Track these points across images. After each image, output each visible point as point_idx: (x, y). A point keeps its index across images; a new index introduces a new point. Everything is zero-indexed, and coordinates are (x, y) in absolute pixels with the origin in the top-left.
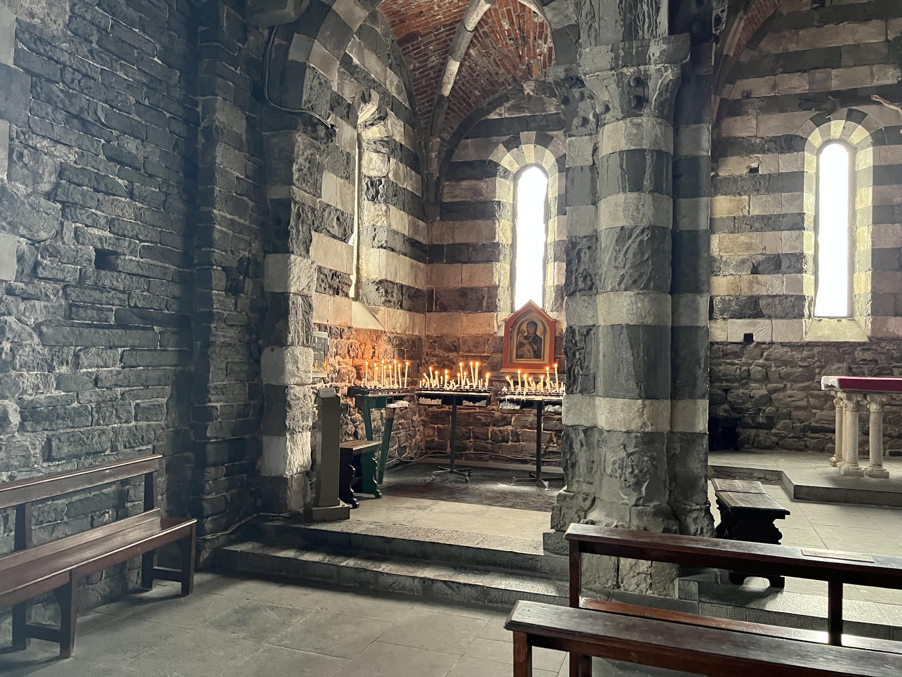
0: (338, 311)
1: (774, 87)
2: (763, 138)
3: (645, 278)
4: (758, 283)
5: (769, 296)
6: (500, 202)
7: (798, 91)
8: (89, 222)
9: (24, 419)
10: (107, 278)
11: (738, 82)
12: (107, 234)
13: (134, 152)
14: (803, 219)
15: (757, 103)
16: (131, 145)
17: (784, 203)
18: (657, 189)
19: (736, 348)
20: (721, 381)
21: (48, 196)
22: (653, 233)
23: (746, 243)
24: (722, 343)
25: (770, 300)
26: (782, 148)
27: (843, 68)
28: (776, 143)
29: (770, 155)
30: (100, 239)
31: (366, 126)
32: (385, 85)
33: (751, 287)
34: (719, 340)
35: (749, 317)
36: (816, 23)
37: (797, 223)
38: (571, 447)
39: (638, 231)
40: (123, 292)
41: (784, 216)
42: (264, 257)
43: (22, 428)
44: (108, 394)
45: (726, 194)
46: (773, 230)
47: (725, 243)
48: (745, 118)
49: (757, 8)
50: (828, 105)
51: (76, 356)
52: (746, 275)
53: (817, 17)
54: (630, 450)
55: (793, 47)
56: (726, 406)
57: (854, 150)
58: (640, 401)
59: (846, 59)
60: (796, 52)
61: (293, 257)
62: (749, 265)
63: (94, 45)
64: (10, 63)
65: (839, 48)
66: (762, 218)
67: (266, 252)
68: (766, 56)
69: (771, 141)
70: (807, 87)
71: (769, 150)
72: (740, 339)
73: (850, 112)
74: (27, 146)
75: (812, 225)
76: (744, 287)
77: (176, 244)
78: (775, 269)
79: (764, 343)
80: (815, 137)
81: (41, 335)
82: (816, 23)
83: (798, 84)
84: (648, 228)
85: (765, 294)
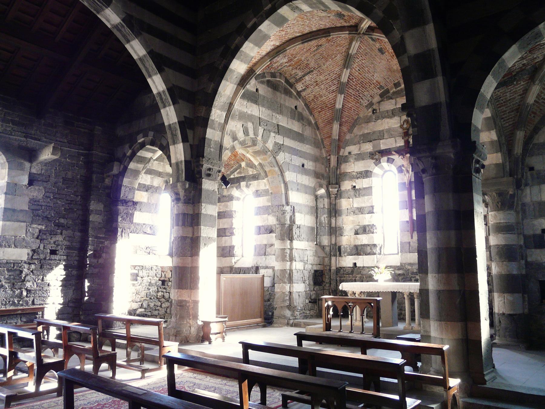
1: (360, 149)
2: (357, 172)
4: (357, 239)
5: (362, 245)
6: (235, 211)
7: (369, 151)
8: (48, 243)
11: (347, 148)
12: (54, 245)
14: (373, 208)
15: (354, 157)
16: (62, 221)
17: (366, 201)
21: (37, 238)
23: (352, 220)
26: (364, 176)
29: (359, 180)
33: (355, 241)
35: (354, 255)
36: (374, 120)
42: (111, 245)
46: (362, 214)
48: (350, 163)
49: (346, 116)
50: (377, 157)
51: (43, 278)
52: (353, 236)
53: (374, 117)
55: (366, 131)
57: (395, 174)
59: (386, 136)
60: (368, 134)
63: (52, 198)
64: (27, 209)
66: (358, 208)
68: (356, 136)
70: (372, 149)
71: (359, 177)
72: (351, 265)
73: (388, 158)
74: (31, 227)
76: (352, 240)
82: (374, 120)
83: (368, 147)
85: (360, 244)
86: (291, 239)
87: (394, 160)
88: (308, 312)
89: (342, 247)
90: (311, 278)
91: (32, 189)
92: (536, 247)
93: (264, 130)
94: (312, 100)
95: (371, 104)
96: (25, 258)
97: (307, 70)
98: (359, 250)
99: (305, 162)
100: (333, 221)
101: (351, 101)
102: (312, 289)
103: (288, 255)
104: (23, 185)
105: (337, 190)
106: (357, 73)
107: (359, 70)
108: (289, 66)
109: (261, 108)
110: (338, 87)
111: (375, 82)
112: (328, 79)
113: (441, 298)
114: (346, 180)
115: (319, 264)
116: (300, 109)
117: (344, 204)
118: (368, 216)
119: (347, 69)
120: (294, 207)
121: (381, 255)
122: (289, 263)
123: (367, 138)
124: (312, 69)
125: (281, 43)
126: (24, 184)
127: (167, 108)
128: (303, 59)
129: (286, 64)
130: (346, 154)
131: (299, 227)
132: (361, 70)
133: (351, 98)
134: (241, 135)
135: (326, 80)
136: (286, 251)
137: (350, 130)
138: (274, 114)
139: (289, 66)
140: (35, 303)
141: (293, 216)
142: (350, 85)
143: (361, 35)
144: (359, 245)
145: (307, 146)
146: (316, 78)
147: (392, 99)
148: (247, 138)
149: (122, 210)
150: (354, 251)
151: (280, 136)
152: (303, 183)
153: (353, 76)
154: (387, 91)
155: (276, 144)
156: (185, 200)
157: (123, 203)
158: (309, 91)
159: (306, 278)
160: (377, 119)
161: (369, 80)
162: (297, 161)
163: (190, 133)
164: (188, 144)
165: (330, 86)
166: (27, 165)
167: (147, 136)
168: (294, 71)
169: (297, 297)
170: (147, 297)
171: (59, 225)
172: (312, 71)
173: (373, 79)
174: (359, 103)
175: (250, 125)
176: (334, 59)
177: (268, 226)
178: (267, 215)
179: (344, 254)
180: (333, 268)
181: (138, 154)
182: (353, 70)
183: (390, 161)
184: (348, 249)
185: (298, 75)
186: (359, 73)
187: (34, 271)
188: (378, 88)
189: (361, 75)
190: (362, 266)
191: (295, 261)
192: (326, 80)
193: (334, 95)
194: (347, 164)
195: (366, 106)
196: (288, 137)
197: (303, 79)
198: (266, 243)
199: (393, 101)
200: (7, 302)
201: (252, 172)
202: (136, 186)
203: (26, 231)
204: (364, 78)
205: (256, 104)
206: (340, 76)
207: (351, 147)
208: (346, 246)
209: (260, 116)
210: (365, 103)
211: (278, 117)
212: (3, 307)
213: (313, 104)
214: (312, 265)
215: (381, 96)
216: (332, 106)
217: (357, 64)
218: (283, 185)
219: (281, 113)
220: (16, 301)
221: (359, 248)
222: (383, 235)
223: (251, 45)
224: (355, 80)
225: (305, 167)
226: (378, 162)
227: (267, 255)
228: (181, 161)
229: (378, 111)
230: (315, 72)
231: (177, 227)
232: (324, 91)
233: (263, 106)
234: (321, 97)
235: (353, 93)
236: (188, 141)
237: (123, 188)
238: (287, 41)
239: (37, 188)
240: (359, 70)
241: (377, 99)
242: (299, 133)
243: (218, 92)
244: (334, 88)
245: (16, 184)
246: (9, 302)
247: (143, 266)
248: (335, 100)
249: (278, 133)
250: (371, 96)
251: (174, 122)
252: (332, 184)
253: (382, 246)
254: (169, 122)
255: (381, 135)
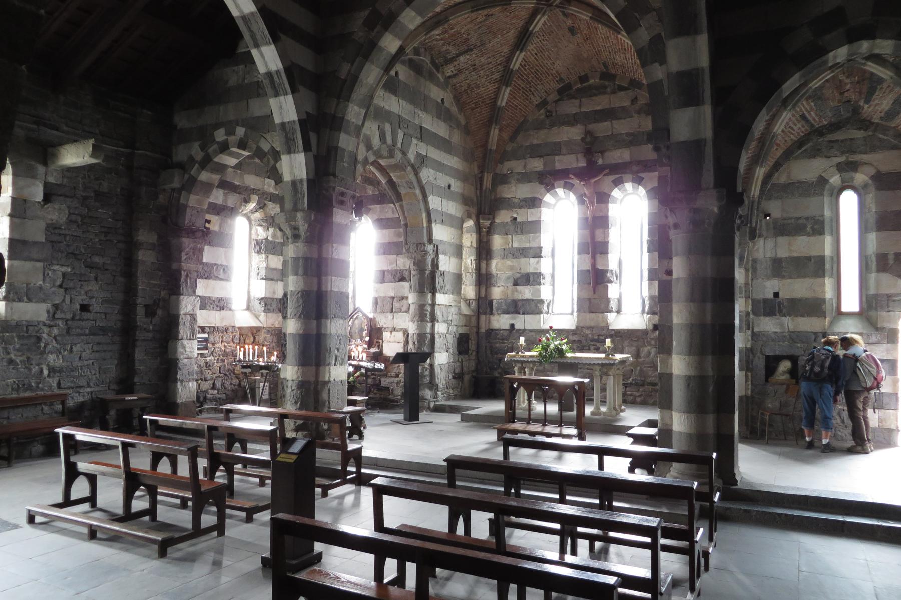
0: (222, 319)
1: (525, 167)
2: (519, 199)
3: (299, 313)
4: (517, 291)
5: (523, 300)
7: (538, 169)
9: (49, 372)
10: (85, 315)
12: (85, 297)
13: (98, 261)
14: (541, 251)
16: (96, 259)
18: (306, 273)
19: (505, 334)
20: (497, 354)
21: (60, 286)
22: (303, 294)
24: (497, 330)
25: (524, 302)
27: (562, 155)
28: (526, 202)
29: (523, 209)
30: (82, 300)
31: (252, 213)
32: (263, 188)
33: (513, 293)
34: (495, 328)
35: (512, 313)
37: (537, 253)
38: (283, 388)
39: (297, 293)
40: (93, 320)
41: (530, 248)
42: (169, 297)
43: (49, 376)
44: (86, 363)
45: (499, 234)
46: (525, 257)
47: (499, 265)
51: (71, 348)
53: (547, 122)
54: (293, 388)
55: (535, 142)
56: (499, 371)
58: (296, 367)
59: (564, 150)
60: (537, 144)
61: (182, 297)
62: (512, 280)
63: (80, 223)
65: (559, 142)
66: (519, 249)
67: (170, 295)
69: (523, 201)
70: (542, 167)
71: (522, 206)
72: (507, 327)
73: (566, 183)
74: (50, 270)
75: (550, 254)
76: (509, 292)
77: (120, 296)
78: (526, 282)
79: (520, 330)
80: (548, 198)
81: (56, 340)
82: (547, 126)
83: (537, 164)
84: (301, 291)
85: (520, 298)
86: (434, 292)
87: (574, 185)
88: (451, 391)
89: (495, 302)
90: (455, 344)
91: (50, 209)
92: (765, 315)
93: (404, 134)
94: (465, 90)
95: (544, 103)
96: (43, 317)
97: (464, 47)
98: (516, 307)
99: (452, 182)
100: (483, 265)
101: (518, 96)
102: (457, 359)
103: (428, 313)
104: (36, 202)
105: (489, 222)
106: (533, 58)
107: (536, 54)
108: (442, 39)
109: (401, 100)
110: (503, 76)
111: (554, 72)
112: (491, 62)
113: (691, 386)
114: (502, 209)
115: (465, 326)
116: (447, 104)
117: (497, 242)
118: (532, 261)
119: (521, 52)
120: (437, 246)
121: (549, 315)
122: (429, 325)
123: (536, 152)
124: (472, 46)
125: (442, 9)
126: (37, 200)
127: (282, 98)
128: (463, 30)
129: (438, 37)
130: (505, 171)
131: (443, 274)
132: (538, 55)
133: (519, 93)
134: (376, 142)
135: (489, 63)
136: (426, 308)
137: (512, 138)
138: (416, 111)
139: (442, 39)
140: (62, 386)
141: (436, 259)
142: (520, 74)
143: (552, 8)
144: (518, 300)
145: (455, 158)
146: (474, 60)
147: (576, 98)
148: (384, 146)
149: (187, 244)
150: (512, 309)
151: (423, 143)
152: (449, 212)
153: (526, 61)
154: (568, 86)
155: (418, 155)
156: (307, 237)
157: (188, 234)
158: (462, 77)
159: (450, 346)
160: (552, 125)
161: (547, 68)
162: (443, 180)
163: (313, 138)
164: (311, 154)
165: (492, 73)
166: (41, 169)
167: (234, 134)
168: (445, 48)
169: (440, 371)
170: (220, 373)
171: (90, 266)
172: (471, 50)
173: (552, 68)
174: (527, 100)
175: (388, 127)
176: (505, 35)
177: (396, 271)
178: (395, 256)
179: (497, 311)
180: (483, 330)
181: (216, 159)
182: (528, 53)
183: (569, 187)
184: (503, 304)
185: (449, 53)
186: (535, 58)
187: (57, 338)
188: (557, 81)
189: (537, 60)
190: (522, 328)
191: (438, 321)
192: (489, 63)
193: (496, 86)
194: (506, 185)
195: (537, 106)
196: (434, 146)
197: (456, 60)
198: (393, 295)
199: (576, 102)
200: (20, 386)
201: (373, 191)
202: (206, 207)
203: (44, 275)
204: (540, 65)
205: (396, 95)
206: (509, 59)
207: (512, 162)
208: (500, 301)
209: (401, 114)
210: (536, 100)
211: (421, 115)
212: (13, 393)
213: (464, 97)
214: (457, 326)
215: (560, 91)
216: (491, 102)
217: (534, 45)
218: (424, 215)
219: (425, 110)
220: (33, 384)
221: (519, 304)
222: (552, 287)
223: (413, 13)
224: (527, 67)
225: (452, 189)
226: (550, 187)
227: (395, 312)
228: (301, 181)
229: (554, 114)
230: (475, 51)
231: (295, 277)
232: (483, 80)
233: (404, 98)
234: (478, 87)
235: (522, 86)
236: (310, 150)
237: (188, 209)
238: (451, 7)
239: (56, 207)
240: (536, 54)
241: (553, 96)
242: (445, 139)
243: (359, 80)
244: (496, 76)
245: (25, 201)
246: (24, 385)
247: (214, 327)
248: (497, 94)
249: (421, 139)
250: (545, 91)
251: (292, 119)
252: (484, 213)
253: (550, 302)
254: (283, 118)
255: (556, 149)
